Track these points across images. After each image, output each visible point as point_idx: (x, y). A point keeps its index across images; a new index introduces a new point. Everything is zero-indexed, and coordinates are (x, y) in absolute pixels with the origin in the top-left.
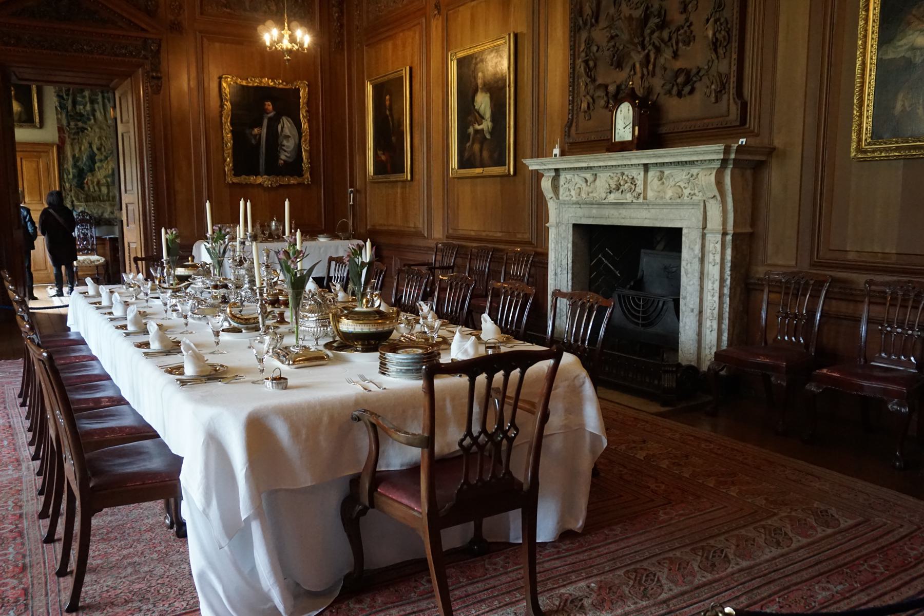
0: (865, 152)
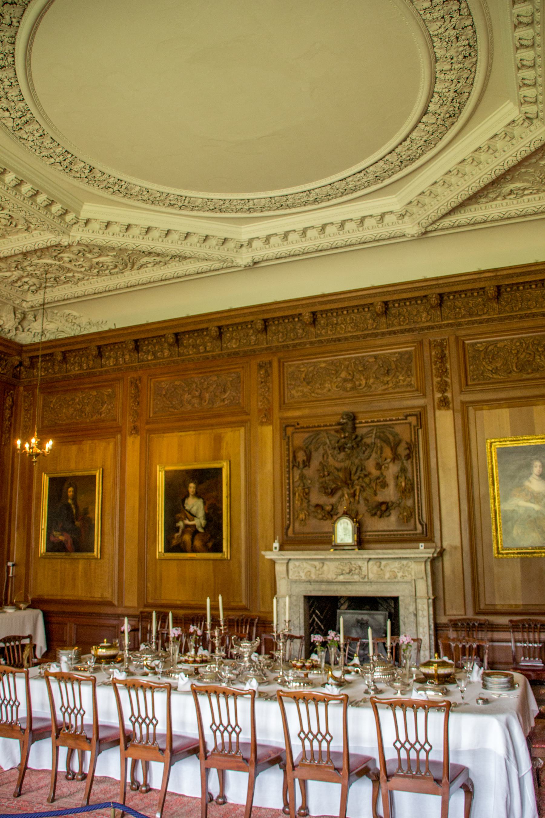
0: (502, 554)
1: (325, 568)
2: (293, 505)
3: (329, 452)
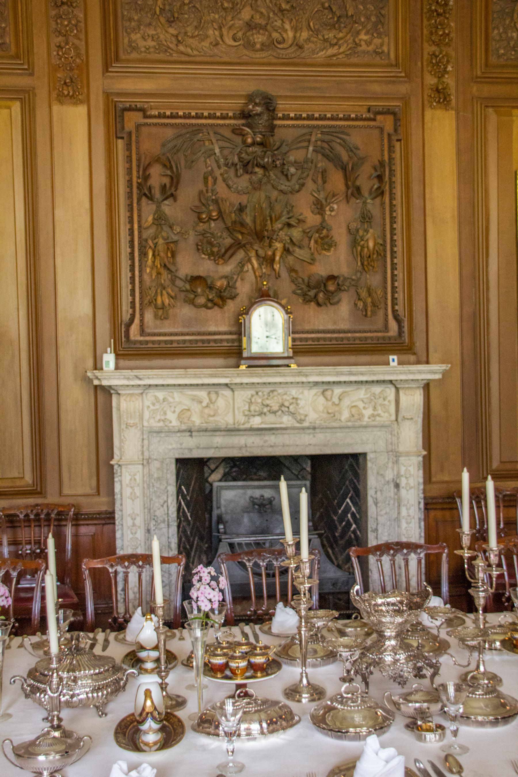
1: (221, 402)
2: (140, 276)
3: (217, 173)
